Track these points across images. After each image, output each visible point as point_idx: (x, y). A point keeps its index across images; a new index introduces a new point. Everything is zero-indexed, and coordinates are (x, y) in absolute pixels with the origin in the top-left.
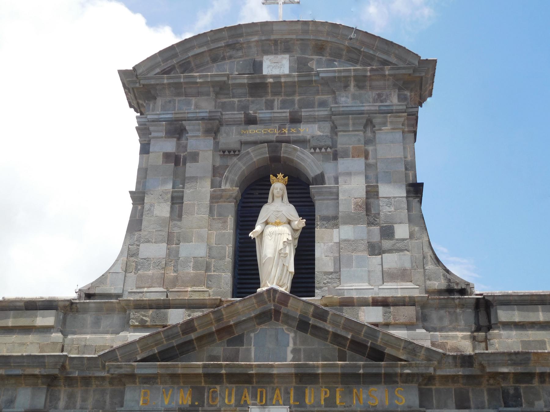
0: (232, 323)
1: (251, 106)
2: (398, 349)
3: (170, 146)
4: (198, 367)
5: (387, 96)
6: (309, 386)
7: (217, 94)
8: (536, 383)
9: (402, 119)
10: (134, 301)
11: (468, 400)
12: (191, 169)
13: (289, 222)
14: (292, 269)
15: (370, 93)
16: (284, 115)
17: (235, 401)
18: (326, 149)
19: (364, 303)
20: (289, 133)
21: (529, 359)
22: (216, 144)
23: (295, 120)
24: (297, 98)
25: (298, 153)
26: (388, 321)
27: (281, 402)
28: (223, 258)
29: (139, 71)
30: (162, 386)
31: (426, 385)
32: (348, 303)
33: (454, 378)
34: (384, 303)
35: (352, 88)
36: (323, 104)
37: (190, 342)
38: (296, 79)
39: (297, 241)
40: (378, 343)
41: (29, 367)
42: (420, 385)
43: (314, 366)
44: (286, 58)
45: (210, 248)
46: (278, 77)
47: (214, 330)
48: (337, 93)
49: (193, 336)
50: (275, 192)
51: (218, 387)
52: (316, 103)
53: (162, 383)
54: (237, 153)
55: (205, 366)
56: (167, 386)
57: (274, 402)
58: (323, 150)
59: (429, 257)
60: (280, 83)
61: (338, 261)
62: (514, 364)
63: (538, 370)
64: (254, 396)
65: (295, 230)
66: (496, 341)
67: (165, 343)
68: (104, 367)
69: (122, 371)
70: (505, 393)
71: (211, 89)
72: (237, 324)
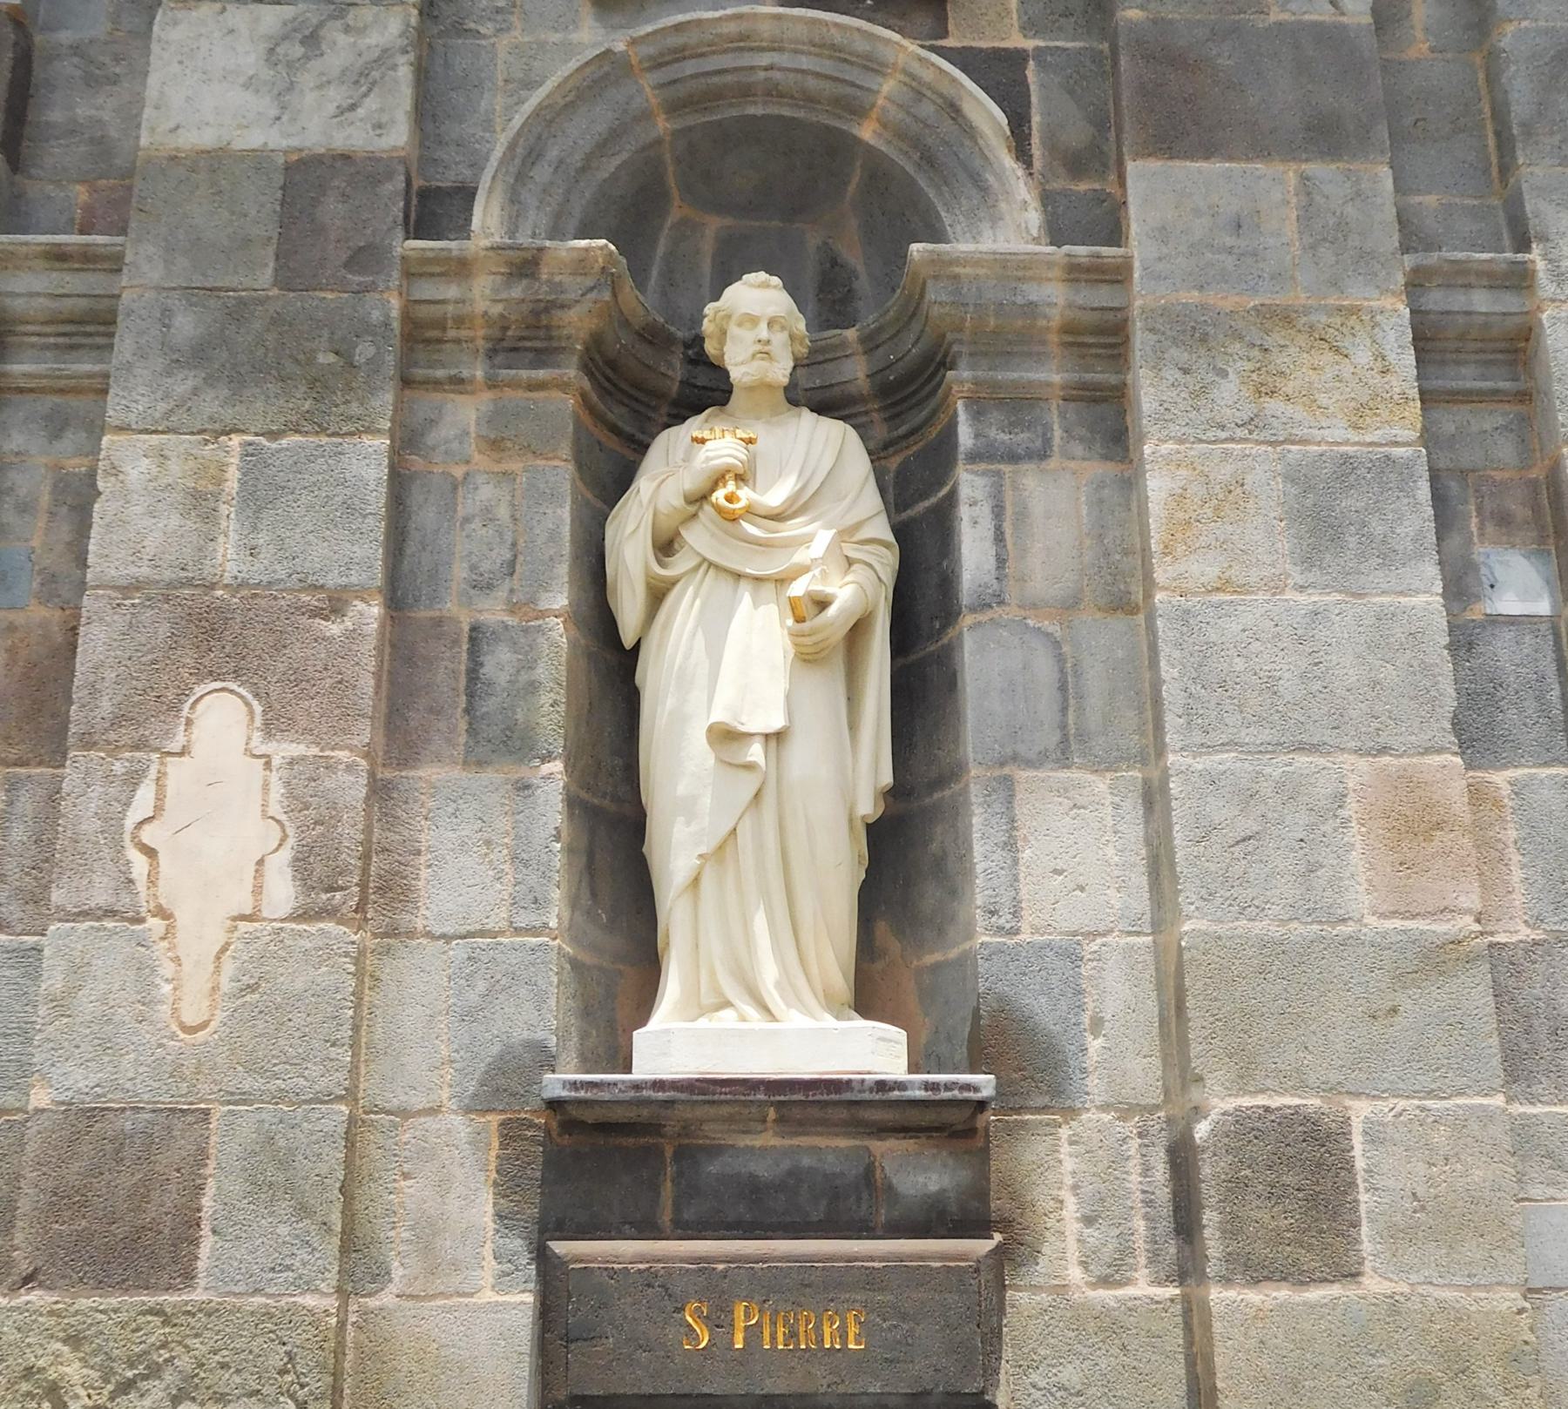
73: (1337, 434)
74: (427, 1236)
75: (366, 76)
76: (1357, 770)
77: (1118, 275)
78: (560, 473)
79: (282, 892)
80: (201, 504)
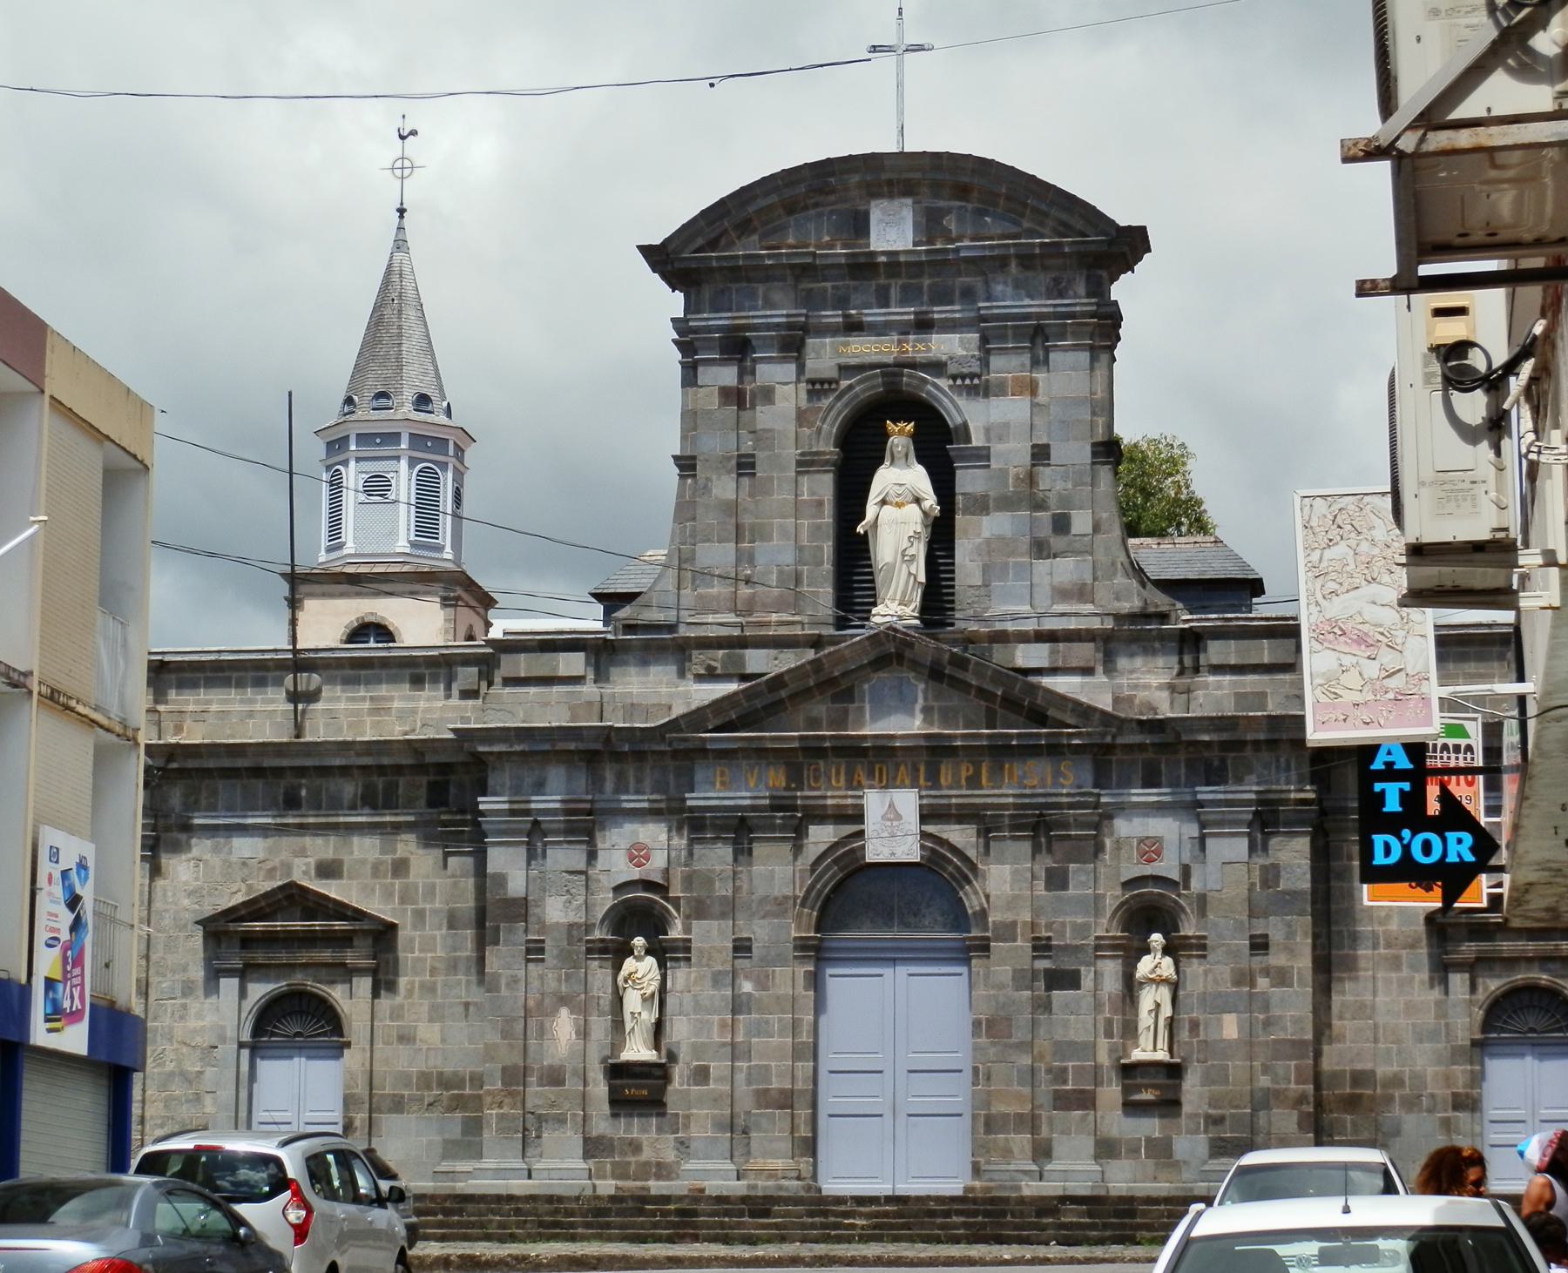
0: (836, 674)
1: (853, 297)
2: (1065, 711)
3: (728, 375)
4: (793, 738)
5: (1069, 281)
6: (945, 760)
7: (797, 279)
8: (1248, 752)
9: (1090, 329)
10: (696, 638)
11: (1159, 773)
12: (764, 416)
13: (918, 501)
14: (922, 578)
15: (1042, 276)
16: (906, 317)
17: (846, 781)
18: (972, 380)
19: (1024, 637)
20: (914, 352)
21: (1238, 724)
22: (801, 369)
23: (924, 325)
24: (927, 282)
25: (929, 387)
26: (1055, 665)
27: (907, 782)
28: (822, 563)
29: (671, 247)
30: (744, 762)
31: (1104, 754)
32: (1001, 637)
33: (1141, 747)
34: (1050, 637)
35: (1013, 267)
36: (968, 295)
37: (781, 701)
38: (924, 258)
39: (930, 529)
40: (1039, 702)
41: (560, 740)
42: (1095, 755)
43: (950, 736)
44: (907, 205)
45: (799, 549)
46: (896, 253)
47: (812, 683)
48: (990, 276)
49: (783, 694)
50: (895, 450)
51: (821, 763)
52: (957, 293)
53: (744, 758)
54: (833, 386)
55: (801, 738)
56: (752, 762)
57: (898, 783)
58: (968, 382)
59: (1119, 565)
60: (899, 264)
61: (986, 569)
62: (1218, 729)
63: (1249, 737)
64: (871, 775)
65: (925, 513)
66: (1200, 692)
67: (745, 704)
68: (663, 738)
69: (689, 745)
70: (1208, 765)
71: (788, 272)
72: (844, 675)
73: (720, 968)
74: (594, 1080)
75: (578, 908)
76: (716, 1018)
77: (689, 940)
78: (609, 971)
79: (574, 1036)
80: (559, 980)
